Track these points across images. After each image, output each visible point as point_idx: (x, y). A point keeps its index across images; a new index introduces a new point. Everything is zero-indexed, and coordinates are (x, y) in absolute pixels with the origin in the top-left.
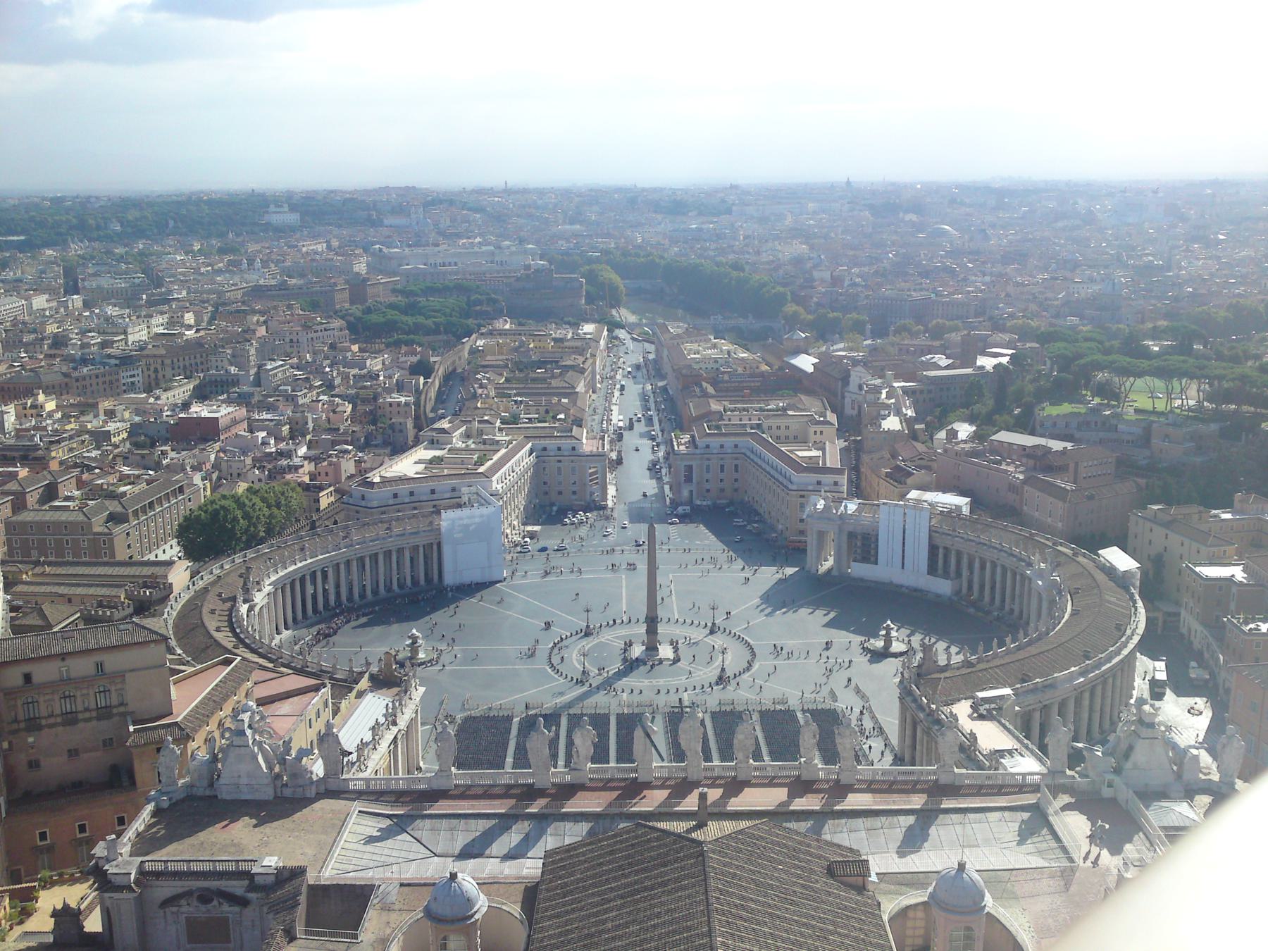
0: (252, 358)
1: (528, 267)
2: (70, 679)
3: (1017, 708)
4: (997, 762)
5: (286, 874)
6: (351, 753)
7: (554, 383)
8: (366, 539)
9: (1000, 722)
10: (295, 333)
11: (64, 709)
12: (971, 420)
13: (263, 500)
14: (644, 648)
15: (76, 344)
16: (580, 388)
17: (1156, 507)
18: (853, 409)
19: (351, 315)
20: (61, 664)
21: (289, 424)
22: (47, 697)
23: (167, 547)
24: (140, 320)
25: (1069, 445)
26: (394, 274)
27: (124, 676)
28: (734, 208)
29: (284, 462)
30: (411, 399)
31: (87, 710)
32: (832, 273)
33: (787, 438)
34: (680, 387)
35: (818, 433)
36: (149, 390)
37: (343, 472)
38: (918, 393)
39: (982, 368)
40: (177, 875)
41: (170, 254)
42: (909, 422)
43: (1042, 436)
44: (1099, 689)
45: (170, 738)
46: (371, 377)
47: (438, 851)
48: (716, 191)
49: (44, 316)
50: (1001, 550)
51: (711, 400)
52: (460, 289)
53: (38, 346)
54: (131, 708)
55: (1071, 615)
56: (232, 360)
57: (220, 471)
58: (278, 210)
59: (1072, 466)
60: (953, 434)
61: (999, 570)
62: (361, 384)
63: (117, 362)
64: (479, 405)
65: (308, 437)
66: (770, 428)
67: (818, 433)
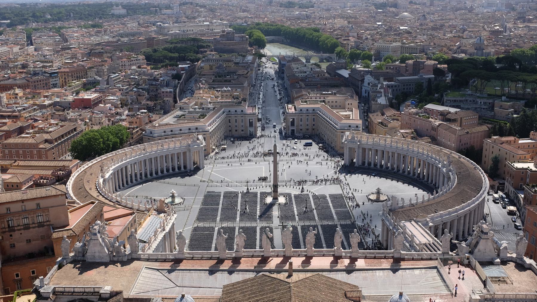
1: (223, 31)
2: (26, 211)
5: (114, 294)
10: (123, 62)
11: (24, 222)
14: (272, 198)
17: (495, 137)
18: (366, 93)
20: (22, 204)
22: (17, 218)
25: (458, 110)
26: (166, 35)
28: (315, 5)
30: (172, 90)
31: (34, 223)
32: (357, 35)
34: (289, 84)
35: (350, 104)
36: (62, 87)
38: (394, 86)
41: (71, 28)
42: (390, 100)
43: (447, 106)
45: (65, 236)
53: (15, 68)
54: (51, 223)
55: (457, 184)
56: (97, 73)
58: (117, 8)
59: (459, 119)
64: (201, 92)
66: (329, 102)
67: (350, 104)
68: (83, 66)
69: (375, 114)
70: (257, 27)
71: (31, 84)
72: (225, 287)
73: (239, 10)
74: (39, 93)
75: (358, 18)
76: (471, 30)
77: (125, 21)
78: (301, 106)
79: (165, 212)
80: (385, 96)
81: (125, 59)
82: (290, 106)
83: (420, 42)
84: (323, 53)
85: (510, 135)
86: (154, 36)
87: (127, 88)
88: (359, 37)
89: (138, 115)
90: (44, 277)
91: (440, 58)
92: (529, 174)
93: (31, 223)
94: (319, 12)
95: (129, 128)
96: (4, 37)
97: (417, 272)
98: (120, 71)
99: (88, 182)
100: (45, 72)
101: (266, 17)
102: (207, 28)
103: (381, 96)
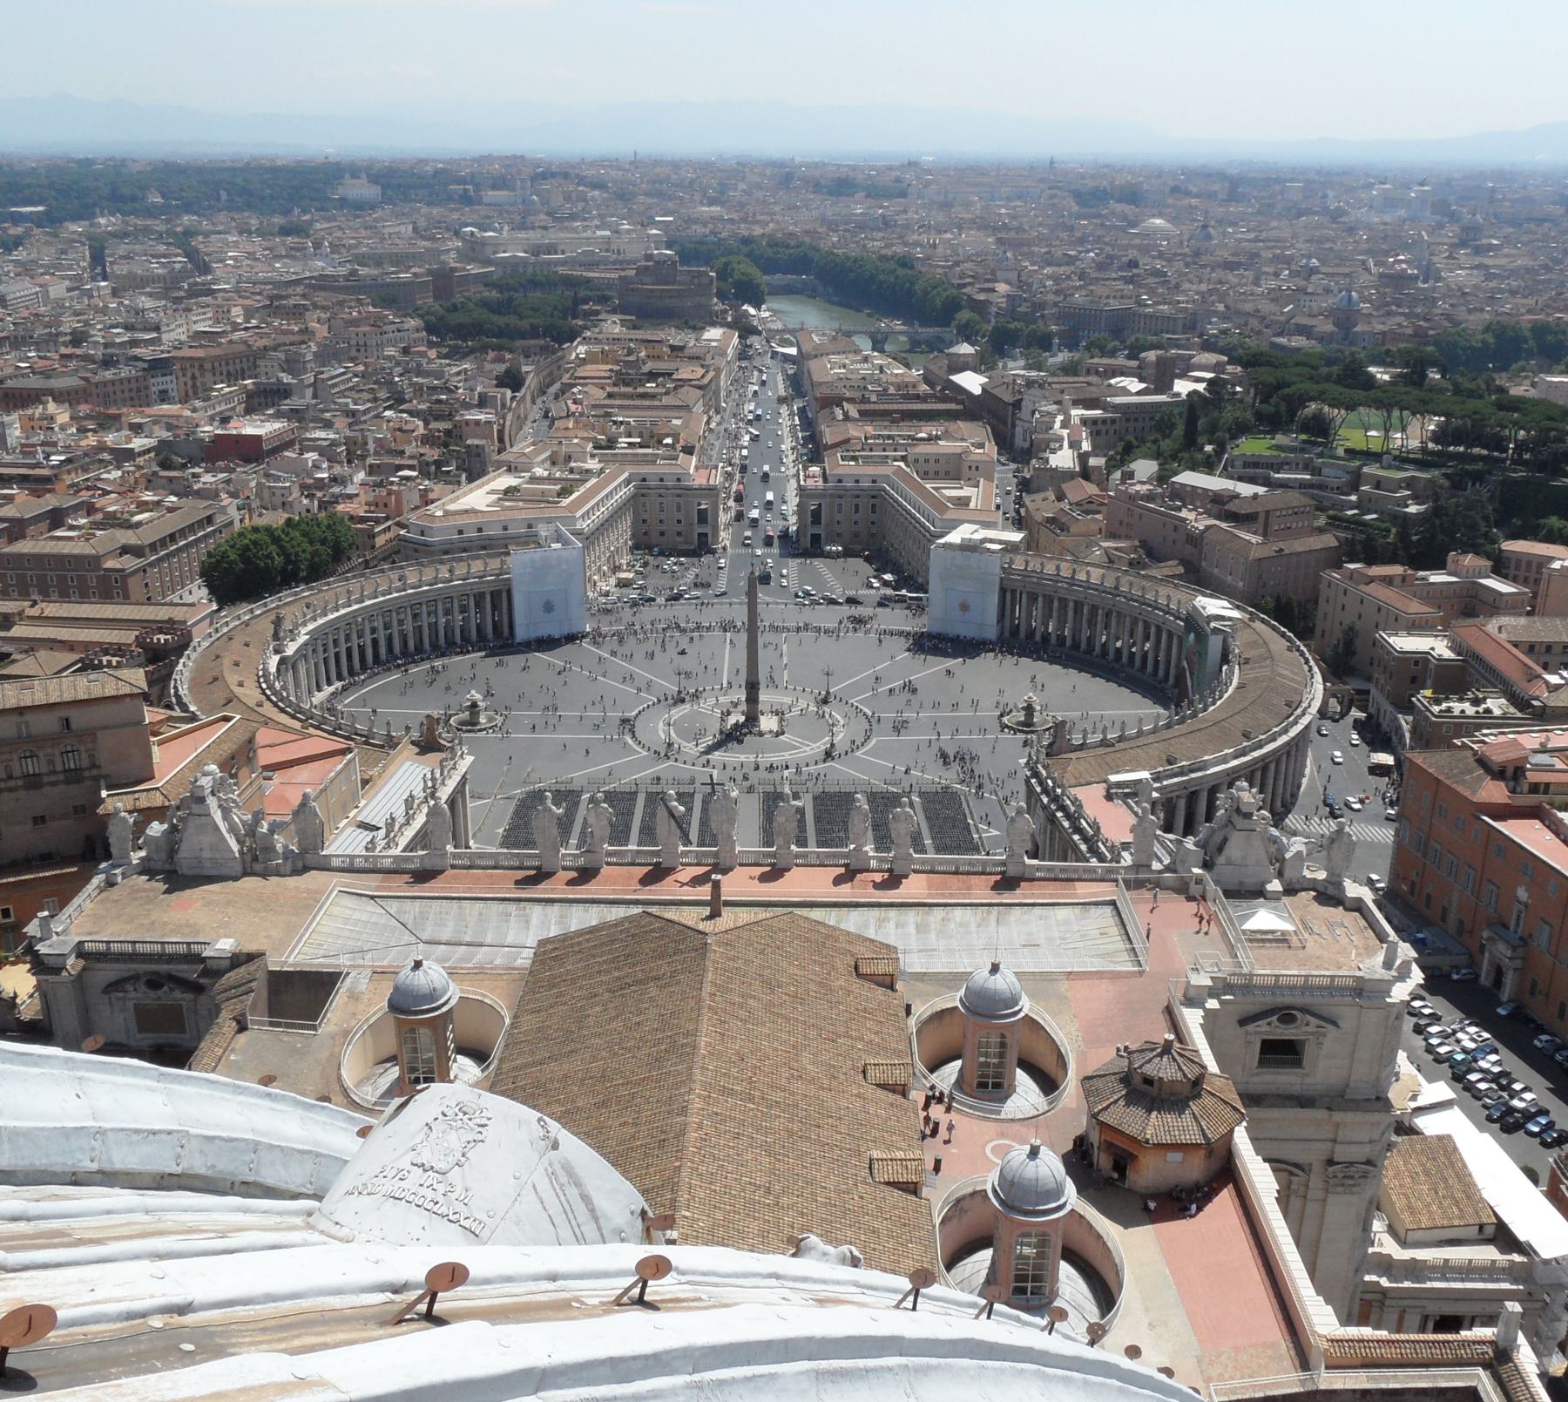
1: (649, 257)
3: (1155, 795)
7: (666, 401)
8: (418, 580)
9: (1131, 808)
12: (1157, 455)
13: (305, 534)
15: (98, 342)
17: (1352, 566)
18: (1025, 440)
20: (19, 719)
21: (345, 444)
24: (177, 315)
25: (1261, 490)
26: (489, 262)
27: (94, 734)
29: (336, 490)
32: (1019, 276)
33: (936, 473)
36: (184, 400)
39: (1178, 395)
42: (1083, 458)
43: (1232, 478)
47: (424, 938)
48: (890, 168)
49: (63, 306)
50: (1167, 613)
52: (569, 282)
57: (262, 499)
60: (1131, 475)
61: (1164, 636)
62: (435, 397)
63: (146, 365)
64: (571, 425)
65: (370, 461)
66: (916, 461)
68: (245, 342)
69: (1041, 495)
70: (745, 249)
71: (95, 391)
72: (542, 943)
73: (697, 197)
74: (117, 418)
75: (1024, 231)
77: (376, 220)
79: (440, 749)
80: (1071, 446)
81: (367, 329)
82: (815, 469)
84: (921, 326)
85: (1392, 560)
86: (453, 265)
87: (368, 410)
88: (1021, 284)
94: (920, 211)
95: (362, 520)
96: (25, 253)
98: (352, 360)
100: (136, 358)
101: (772, 221)
102: (604, 247)
103: (1061, 447)
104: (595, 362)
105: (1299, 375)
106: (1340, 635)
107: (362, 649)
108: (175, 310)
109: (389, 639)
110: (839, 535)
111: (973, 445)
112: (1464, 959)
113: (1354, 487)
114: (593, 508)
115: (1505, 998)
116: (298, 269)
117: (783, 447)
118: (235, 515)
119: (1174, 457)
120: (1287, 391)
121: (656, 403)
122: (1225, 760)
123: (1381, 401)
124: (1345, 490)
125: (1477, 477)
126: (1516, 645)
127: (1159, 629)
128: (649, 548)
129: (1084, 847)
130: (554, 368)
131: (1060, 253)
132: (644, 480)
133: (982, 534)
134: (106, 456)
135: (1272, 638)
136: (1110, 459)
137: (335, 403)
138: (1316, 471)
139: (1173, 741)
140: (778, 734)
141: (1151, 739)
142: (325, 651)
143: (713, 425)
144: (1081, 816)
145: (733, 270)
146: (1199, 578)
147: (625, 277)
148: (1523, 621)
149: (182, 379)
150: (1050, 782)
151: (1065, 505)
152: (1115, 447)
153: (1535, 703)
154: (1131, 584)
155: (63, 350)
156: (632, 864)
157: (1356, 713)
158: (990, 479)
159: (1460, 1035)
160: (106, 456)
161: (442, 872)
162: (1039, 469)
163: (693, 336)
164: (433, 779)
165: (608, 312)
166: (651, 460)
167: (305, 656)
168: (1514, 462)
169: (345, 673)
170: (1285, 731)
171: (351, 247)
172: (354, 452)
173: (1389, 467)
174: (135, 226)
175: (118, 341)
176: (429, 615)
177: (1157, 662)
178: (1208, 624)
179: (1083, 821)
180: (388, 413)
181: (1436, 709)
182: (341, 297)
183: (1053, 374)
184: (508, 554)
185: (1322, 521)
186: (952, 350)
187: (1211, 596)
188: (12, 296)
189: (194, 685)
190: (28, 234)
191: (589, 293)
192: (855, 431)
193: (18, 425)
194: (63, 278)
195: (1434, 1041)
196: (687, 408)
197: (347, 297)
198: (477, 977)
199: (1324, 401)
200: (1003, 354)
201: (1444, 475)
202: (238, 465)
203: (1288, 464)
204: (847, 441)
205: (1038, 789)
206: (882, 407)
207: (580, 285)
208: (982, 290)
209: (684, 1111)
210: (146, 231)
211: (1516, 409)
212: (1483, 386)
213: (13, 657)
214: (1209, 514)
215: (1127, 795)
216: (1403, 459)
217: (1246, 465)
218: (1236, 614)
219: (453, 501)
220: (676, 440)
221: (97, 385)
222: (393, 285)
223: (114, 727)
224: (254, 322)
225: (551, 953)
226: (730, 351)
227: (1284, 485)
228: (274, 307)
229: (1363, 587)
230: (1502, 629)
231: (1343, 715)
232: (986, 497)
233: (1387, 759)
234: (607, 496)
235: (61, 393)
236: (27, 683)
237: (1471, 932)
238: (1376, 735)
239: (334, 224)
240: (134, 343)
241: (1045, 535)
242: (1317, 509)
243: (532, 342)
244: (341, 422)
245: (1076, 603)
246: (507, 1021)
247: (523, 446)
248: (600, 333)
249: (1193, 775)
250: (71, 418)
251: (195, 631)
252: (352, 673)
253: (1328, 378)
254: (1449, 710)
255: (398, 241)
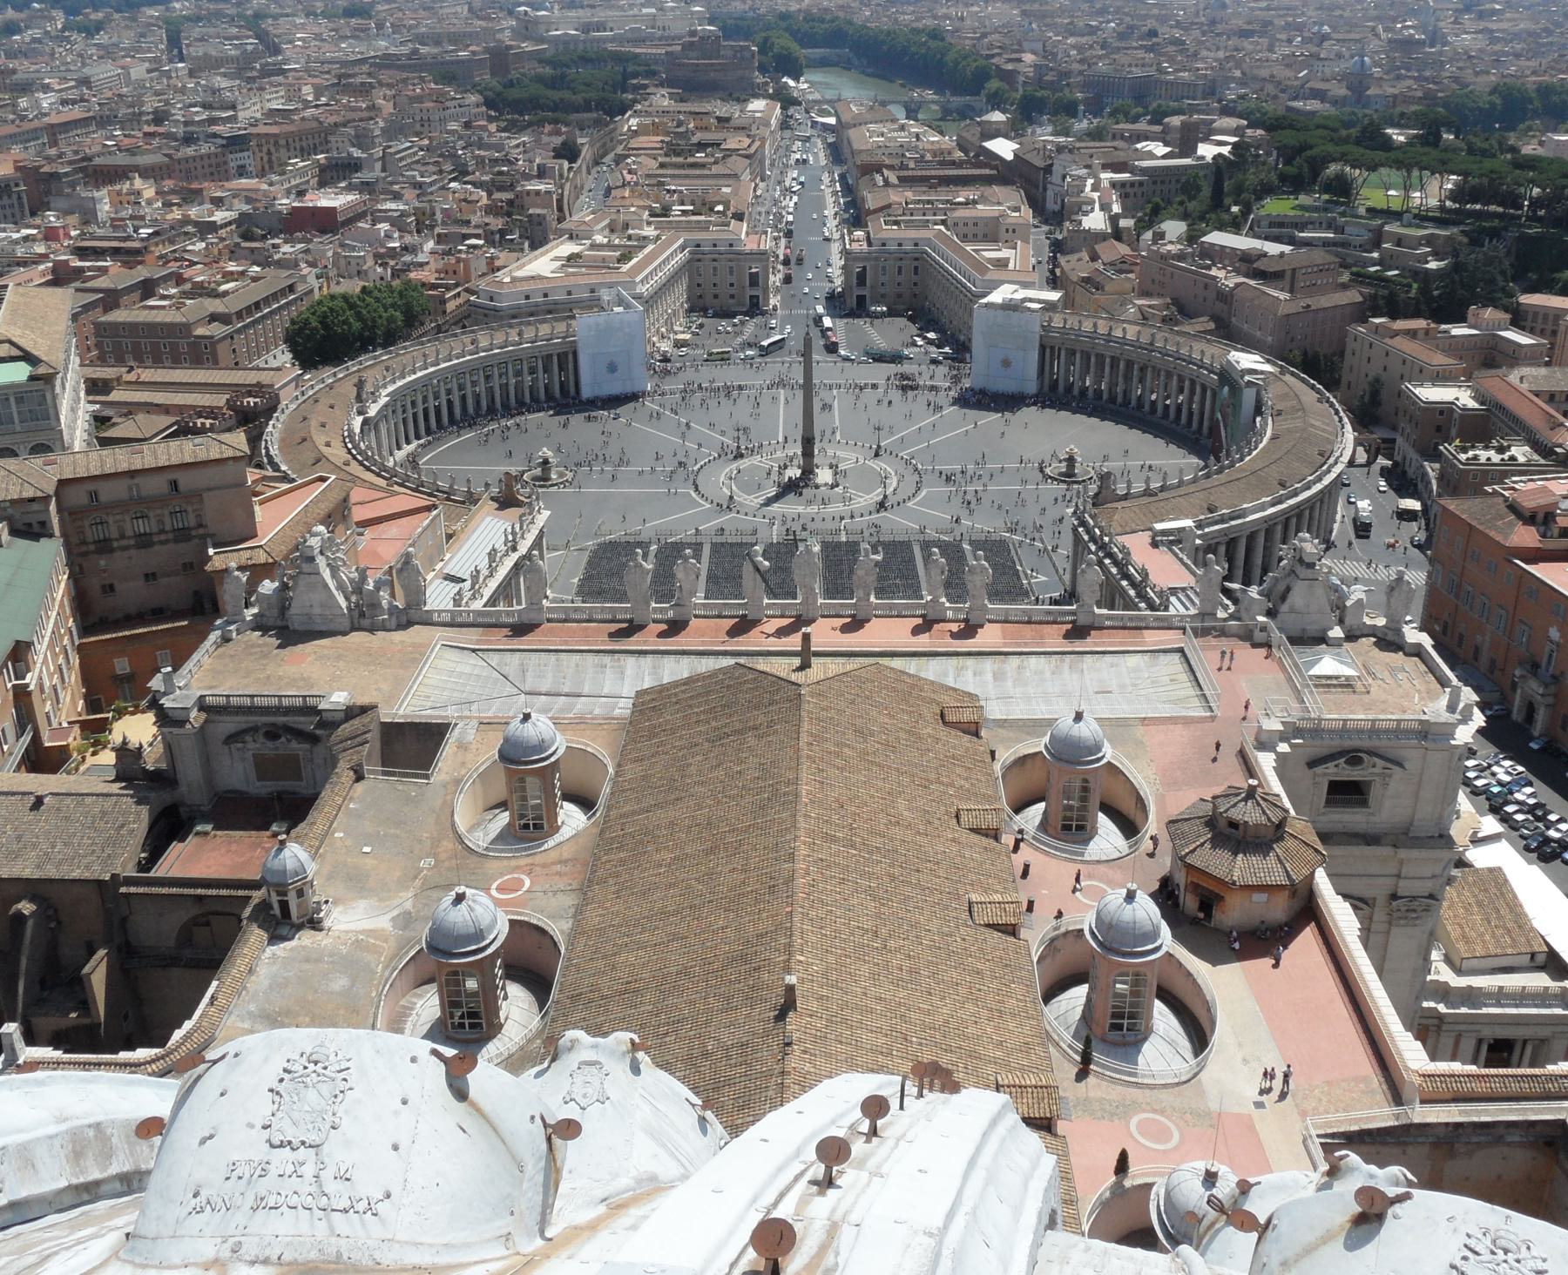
0: (377, 141)
1: (693, 33)
3: (1198, 542)
4: (1168, 599)
6: (464, 581)
7: (715, 170)
8: (488, 343)
9: (1176, 555)
12: (1184, 216)
16: (746, 176)
17: (1377, 320)
18: (1056, 203)
19: (490, 90)
22: (118, 517)
23: (277, 352)
24: (252, 93)
25: (1287, 249)
26: (542, 40)
29: (408, 258)
31: (162, 531)
32: (1044, 46)
33: (975, 236)
36: (262, 174)
37: (473, 270)
39: (1203, 158)
40: (241, 710)
41: (287, 15)
42: (1114, 219)
43: (1259, 237)
44: (1294, 520)
46: (508, 160)
51: (890, 190)
52: (619, 58)
57: (338, 269)
59: (1288, 275)
60: (1161, 235)
61: (1198, 389)
62: (497, 169)
65: (438, 230)
66: (956, 224)
68: (317, 119)
69: (1076, 256)
71: (177, 167)
72: (639, 694)
74: (199, 192)
76: (1340, 36)
78: (883, 235)
79: (519, 504)
80: (1102, 209)
81: (431, 104)
82: (859, 234)
83: (1206, 69)
84: (953, 94)
85: (1416, 314)
87: (434, 182)
88: (1047, 53)
89: (460, 251)
90: (175, 670)
91: (1252, 112)
92: (1456, 416)
93: (155, 530)
95: (434, 287)
96: (106, 37)
97: (1133, 660)
98: (417, 134)
99: (323, 426)
100: (215, 135)
103: (1092, 210)
104: (647, 134)
105: (1321, 137)
106: (1367, 387)
107: (438, 410)
108: (250, 89)
109: (463, 398)
110: (883, 296)
111: (1009, 208)
112: (1496, 696)
113: (1376, 244)
114: (651, 273)
115: (1536, 733)
116: (363, 49)
117: (826, 213)
118: (313, 282)
119: (1202, 218)
120: (1309, 153)
121: (706, 172)
122: (1263, 507)
123: (1402, 162)
124: (1367, 247)
125: (1494, 234)
126: (1537, 395)
127: (1193, 383)
128: (704, 311)
129: (1132, 593)
130: (607, 139)
131: (1081, 24)
132: (698, 246)
133: (1021, 294)
134: (190, 229)
135: (1303, 390)
136: (1139, 220)
137: (403, 176)
138: (1340, 230)
139: (1213, 490)
140: (832, 487)
141: (1192, 488)
142: (404, 412)
143: (759, 193)
144: (1129, 563)
145: (773, 44)
146: (1229, 333)
147: (672, 53)
148: (1543, 371)
149: (259, 155)
150: (1097, 530)
151: (1099, 265)
152: (1142, 209)
153: (1558, 450)
154: (1166, 340)
155: (146, 129)
156: (719, 617)
157: (1383, 461)
158: (1026, 241)
159: (1495, 769)
160: (190, 229)
161: (538, 626)
162: (1073, 231)
163: (737, 107)
164: (514, 533)
165: (656, 86)
166: (704, 227)
167: (385, 416)
168: (1529, 218)
169: (423, 432)
170: (1319, 479)
171: (411, 27)
172: (423, 221)
173: (1409, 225)
174: (208, 9)
175: (197, 119)
176: (500, 376)
177: (1191, 414)
178: (1242, 377)
179: (1130, 567)
180: (452, 185)
181: (1463, 457)
182: (405, 75)
183: (1080, 140)
184: (573, 317)
185: (1345, 277)
186: (985, 118)
187: (1242, 350)
188: (96, 78)
189: (284, 445)
190: (108, 18)
191: (638, 69)
192: (896, 197)
193: (107, 200)
194: (143, 60)
195: (1471, 775)
196: (735, 176)
197: (411, 75)
198: (578, 727)
199: (1346, 162)
200: (1031, 121)
201: (1462, 232)
202: (315, 236)
203: (1311, 223)
204: (889, 206)
205: (1086, 537)
206: (919, 173)
207: (627, 61)
208: (1010, 60)
209: (791, 858)
210: (218, 15)
211: (1533, 168)
212: (1496, 146)
213: (113, 420)
214: (1238, 272)
215: (1171, 542)
216: (1422, 218)
217: (1271, 225)
218: (1268, 368)
219: (519, 268)
220: (727, 207)
221: (179, 161)
222: (452, 62)
223: (219, 488)
224: (324, 100)
225: (649, 703)
226: (773, 121)
227: (1308, 243)
228: (342, 85)
229: (1387, 340)
230: (1523, 381)
231: (1369, 464)
232: (1024, 257)
233: (1413, 504)
234: (664, 262)
235: (146, 169)
236: (136, 446)
237: (1503, 670)
238: (1402, 482)
239: (393, 6)
240: (212, 121)
241: (1080, 294)
242: (1341, 266)
243: (586, 115)
244: (409, 194)
245: (1112, 358)
246: (611, 770)
247: (582, 215)
248: (651, 105)
249: (1233, 523)
250: (157, 193)
251: (282, 394)
252: (429, 432)
253: (1346, 141)
254: (1476, 458)
255: (456, 21)
